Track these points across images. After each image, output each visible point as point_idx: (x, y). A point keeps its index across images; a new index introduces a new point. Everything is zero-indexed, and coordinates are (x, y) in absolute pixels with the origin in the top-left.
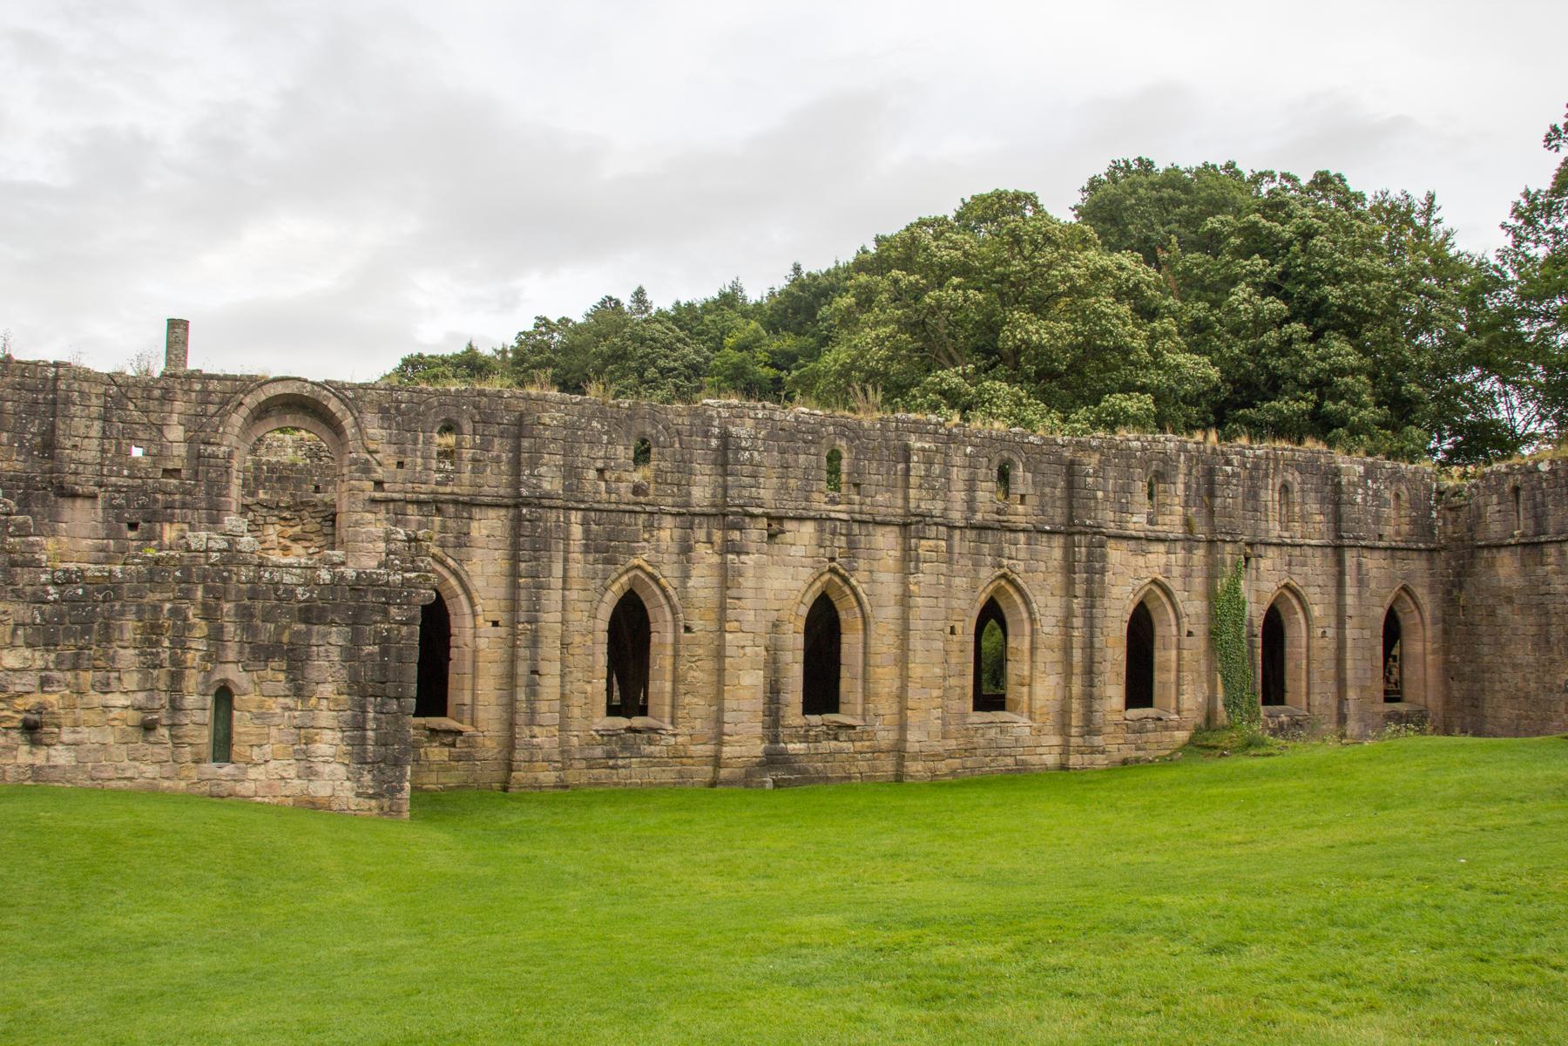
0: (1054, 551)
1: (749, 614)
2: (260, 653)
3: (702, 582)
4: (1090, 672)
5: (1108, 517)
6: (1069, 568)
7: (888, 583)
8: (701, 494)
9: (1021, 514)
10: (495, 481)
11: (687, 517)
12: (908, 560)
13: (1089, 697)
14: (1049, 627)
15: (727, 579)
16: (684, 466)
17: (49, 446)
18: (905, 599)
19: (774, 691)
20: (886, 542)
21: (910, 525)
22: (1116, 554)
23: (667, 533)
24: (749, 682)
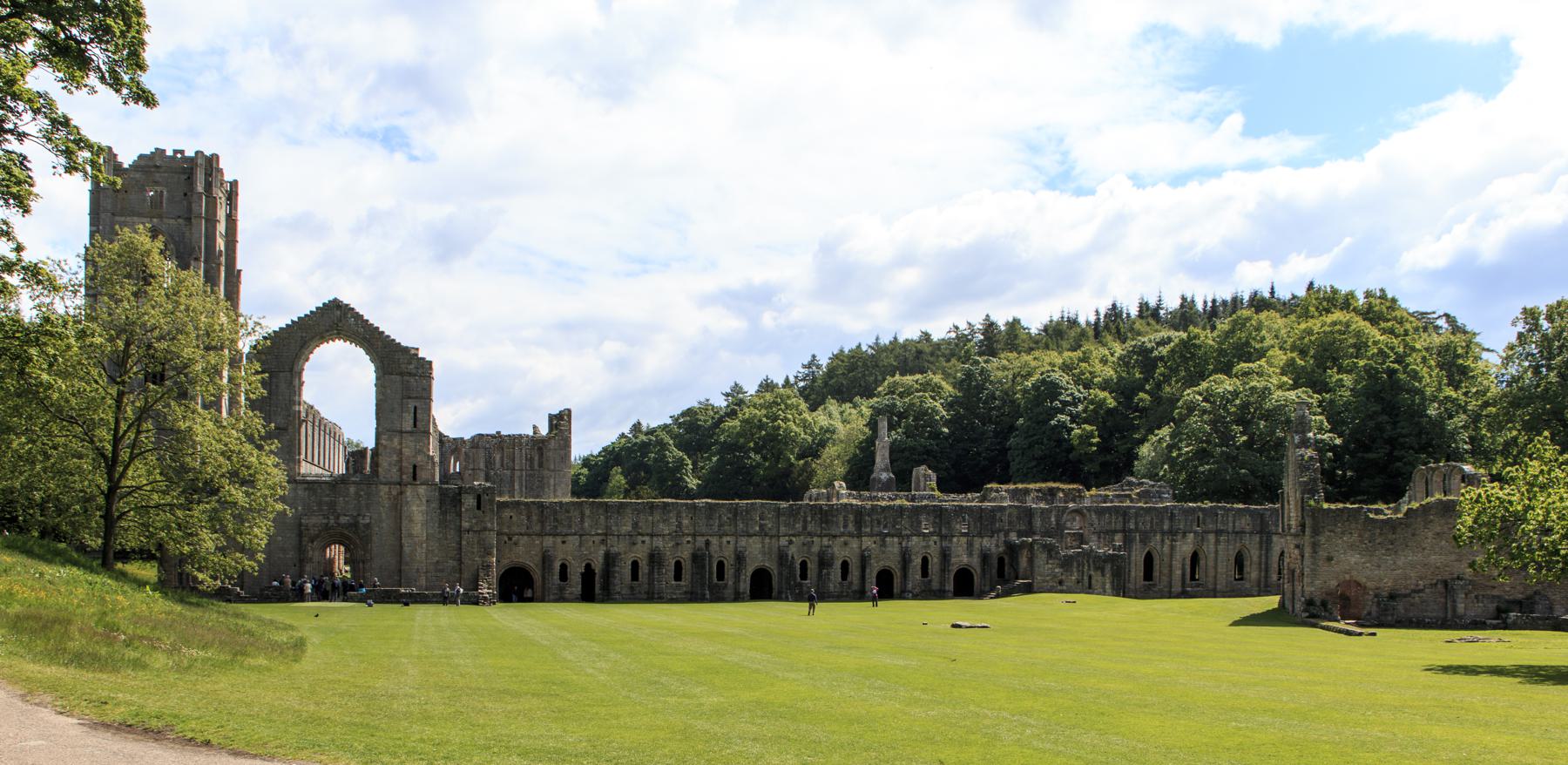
0: (1257, 538)
1: (1178, 556)
2: (1097, 569)
3: (1166, 549)
4: (1267, 571)
5: (1273, 528)
6: (1261, 543)
7: (1212, 547)
8: (1166, 527)
9: (1248, 529)
10: (1120, 526)
11: (1163, 533)
12: (1217, 542)
13: (1266, 577)
14: (1255, 559)
15: (1172, 548)
16: (1162, 521)
17: (1030, 523)
18: (1216, 552)
19: (1183, 575)
20: (1212, 537)
21: (1218, 533)
22: (1275, 538)
23: (1158, 537)
24: (1179, 572)
